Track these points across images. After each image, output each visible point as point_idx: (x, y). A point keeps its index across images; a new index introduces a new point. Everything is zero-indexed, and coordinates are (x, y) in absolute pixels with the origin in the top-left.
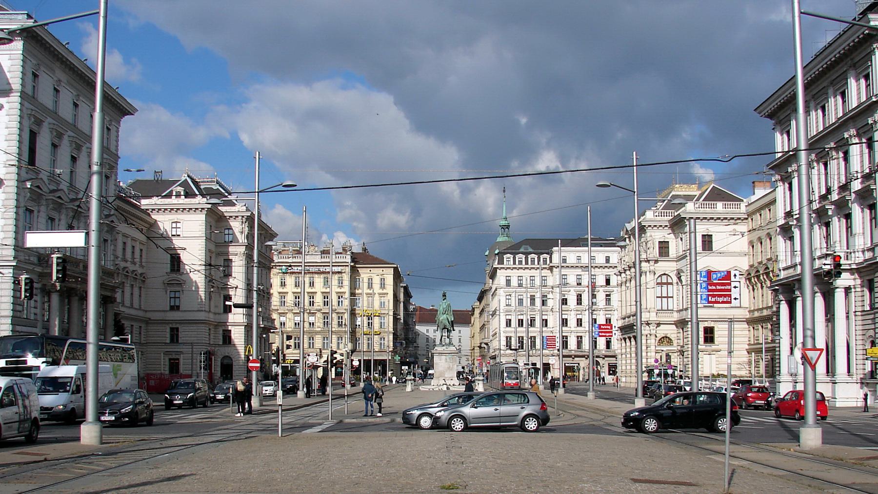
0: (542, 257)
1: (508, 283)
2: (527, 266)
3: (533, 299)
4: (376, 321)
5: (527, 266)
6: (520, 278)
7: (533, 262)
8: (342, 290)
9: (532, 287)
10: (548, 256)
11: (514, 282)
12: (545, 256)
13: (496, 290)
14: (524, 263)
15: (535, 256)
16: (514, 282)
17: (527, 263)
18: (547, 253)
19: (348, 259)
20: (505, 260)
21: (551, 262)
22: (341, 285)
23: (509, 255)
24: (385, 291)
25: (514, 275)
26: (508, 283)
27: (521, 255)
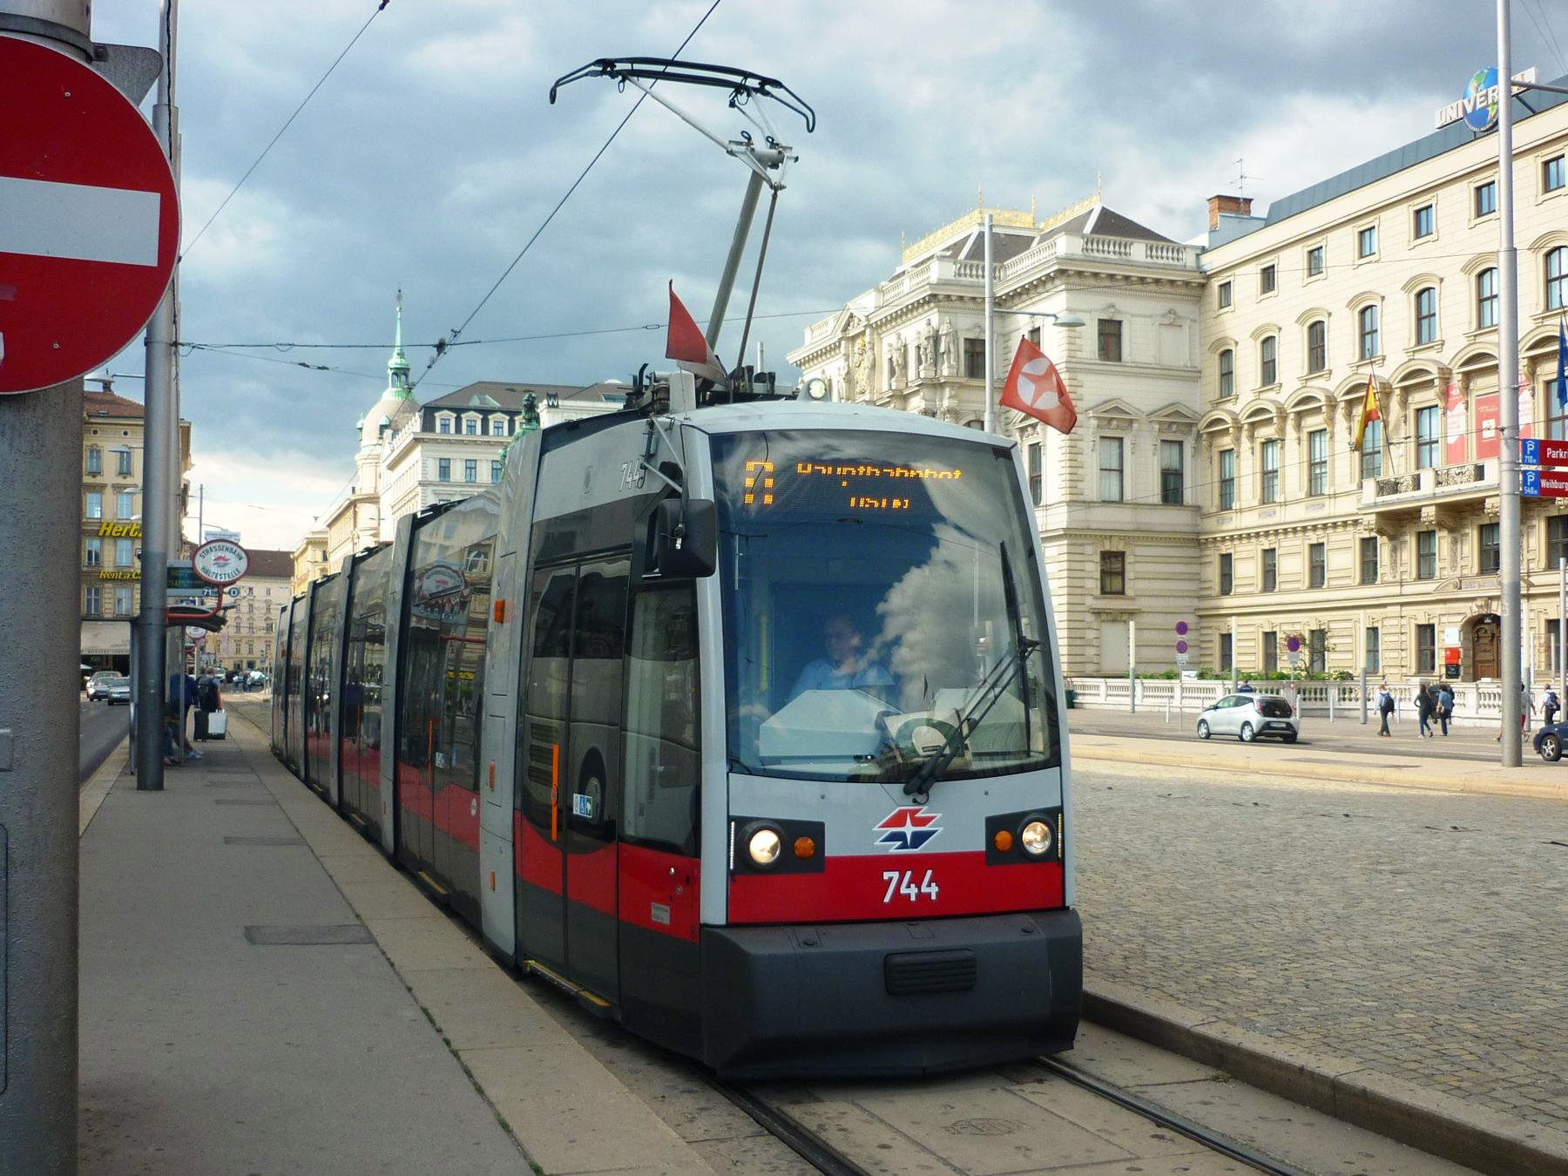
2: (485, 438)
5: (485, 438)
27: (472, 414)
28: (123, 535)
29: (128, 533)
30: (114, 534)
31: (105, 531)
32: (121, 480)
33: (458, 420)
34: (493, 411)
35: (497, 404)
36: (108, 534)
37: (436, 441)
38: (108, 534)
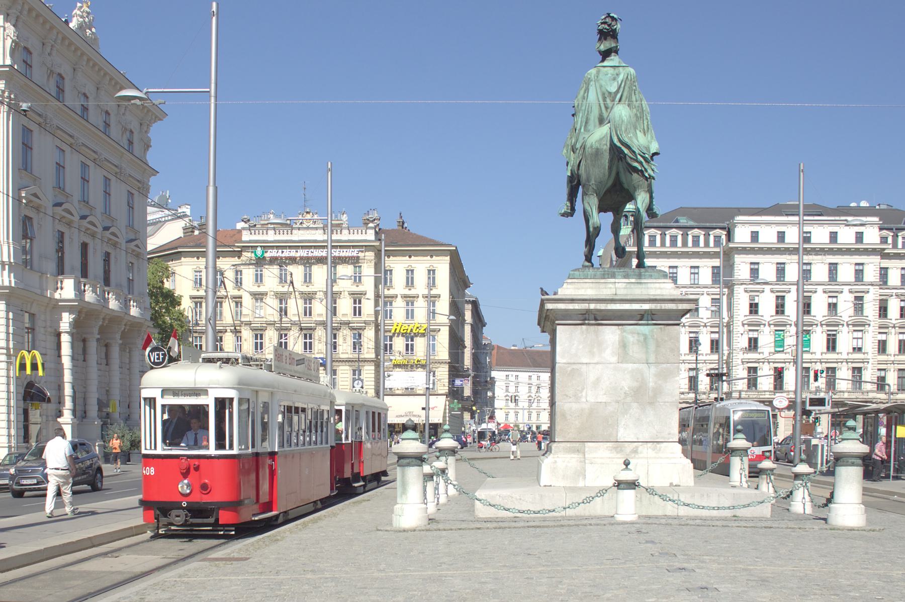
4: (420, 344)
7: (696, 242)
8: (361, 288)
9: (695, 285)
12: (718, 232)
15: (701, 233)
18: (723, 228)
19: (370, 235)
22: (357, 279)
24: (434, 292)
28: (408, 332)
29: (412, 330)
30: (402, 331)
31: (396, 329)
32: (407, 292)
33: (663, 236)
35: (691, 223)
36: (397, 331)
38: (397, 331)
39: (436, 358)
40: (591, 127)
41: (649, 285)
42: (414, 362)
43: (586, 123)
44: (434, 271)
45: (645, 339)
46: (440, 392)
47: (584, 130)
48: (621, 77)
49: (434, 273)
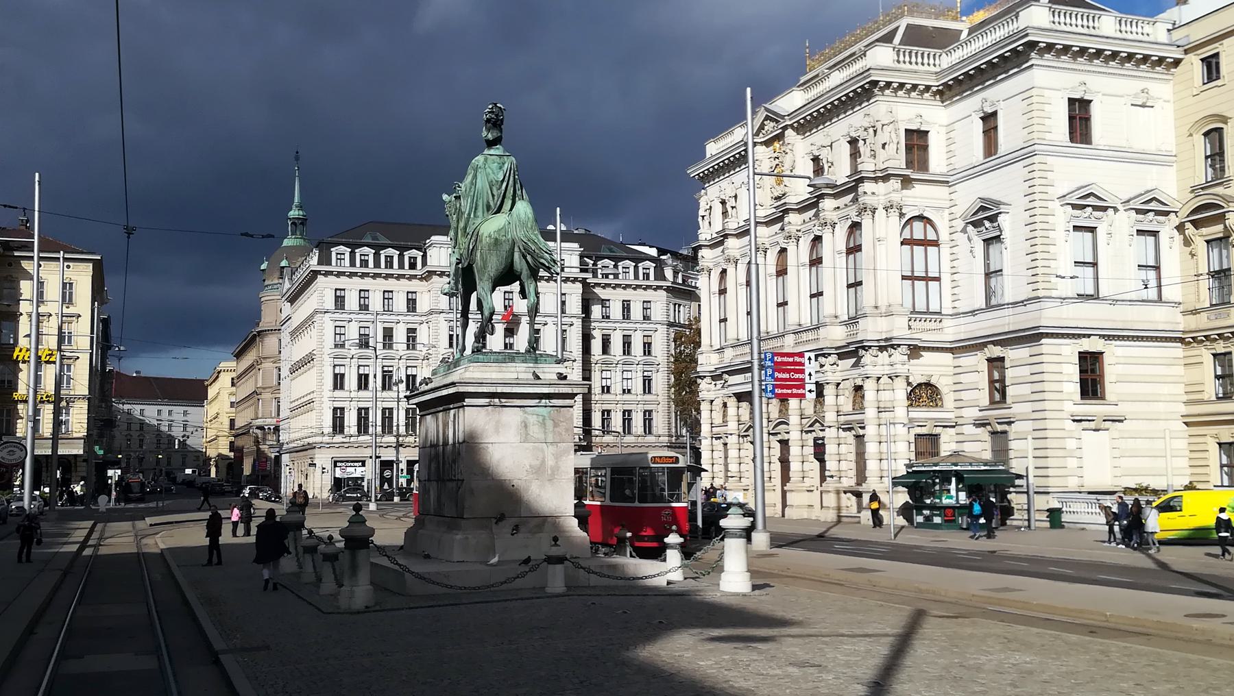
0: (407, 254)
1: (340, 301)
2: (377, 271)
3: (388, 334)
6: (363, 294)
7: (389, 264)
10: (418, 254)
11: (352, 302)
12: (414, 252)
13: (316, 312)
14: (371, 264)
15: (395, 253)
16: (352, 302)
17: (377, 265)
18: (419, 249)
20: (334, 255)
21: (424, 263)
23: (342, 248)
24: (72, 310)
25: (352, 287)
26: (340, 301)
27: (366, 250)
34: (385, 247)
37: (331, 273)
39: (72, 393)
40: (480, 213)
41: (546, 370)
42: (42, 398)
43: (476, 209)
44: (71, 284)
45: (544, 420)
46: (75, 435)
47: (474, 216)
48: (506, 165)
49: (71, 288)
